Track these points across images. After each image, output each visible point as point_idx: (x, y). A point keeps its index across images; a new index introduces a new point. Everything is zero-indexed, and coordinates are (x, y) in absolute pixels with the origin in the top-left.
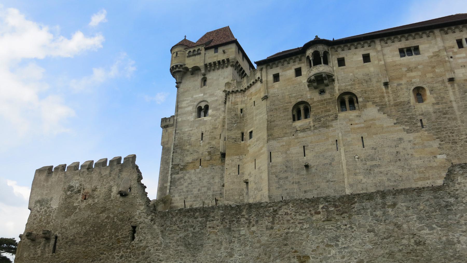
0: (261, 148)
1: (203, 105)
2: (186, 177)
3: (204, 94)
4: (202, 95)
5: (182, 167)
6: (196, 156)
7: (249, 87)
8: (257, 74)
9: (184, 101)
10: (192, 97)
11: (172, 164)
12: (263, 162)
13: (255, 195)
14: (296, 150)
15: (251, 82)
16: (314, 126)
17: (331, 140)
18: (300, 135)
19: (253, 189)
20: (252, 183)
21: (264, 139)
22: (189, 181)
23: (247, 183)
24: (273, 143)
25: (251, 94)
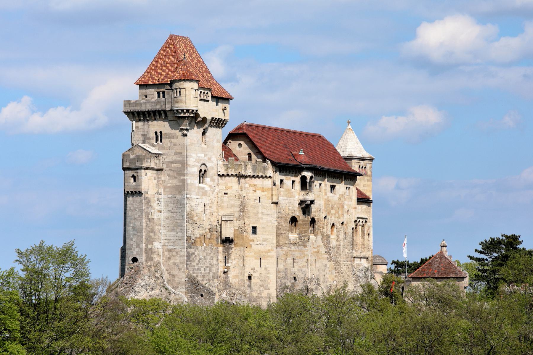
0: (269, 251)
1: (203, 168)
2: (196, 254)
3: (205, 155)
4: (203, 155)
5: (193, 241)
6: (201, 232)
7: (253, 176)
8: (269, 171)
9: (192, 157)
10: (197, 154)
11: (186, 236)
12: (270, 264)
13: (260, 291)
14: (290, 261)
15: (260, 175)
16: (299, 242)
17: (306, 258)
18: (293, 248)
19: (258, 285)
20: (256, 278)
21: (273, 243)
22: (198, 259)
23: (250, 278)
24: (279, 249)
25: (255, 185)
